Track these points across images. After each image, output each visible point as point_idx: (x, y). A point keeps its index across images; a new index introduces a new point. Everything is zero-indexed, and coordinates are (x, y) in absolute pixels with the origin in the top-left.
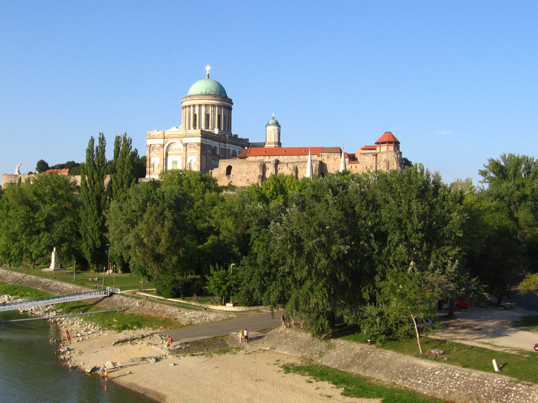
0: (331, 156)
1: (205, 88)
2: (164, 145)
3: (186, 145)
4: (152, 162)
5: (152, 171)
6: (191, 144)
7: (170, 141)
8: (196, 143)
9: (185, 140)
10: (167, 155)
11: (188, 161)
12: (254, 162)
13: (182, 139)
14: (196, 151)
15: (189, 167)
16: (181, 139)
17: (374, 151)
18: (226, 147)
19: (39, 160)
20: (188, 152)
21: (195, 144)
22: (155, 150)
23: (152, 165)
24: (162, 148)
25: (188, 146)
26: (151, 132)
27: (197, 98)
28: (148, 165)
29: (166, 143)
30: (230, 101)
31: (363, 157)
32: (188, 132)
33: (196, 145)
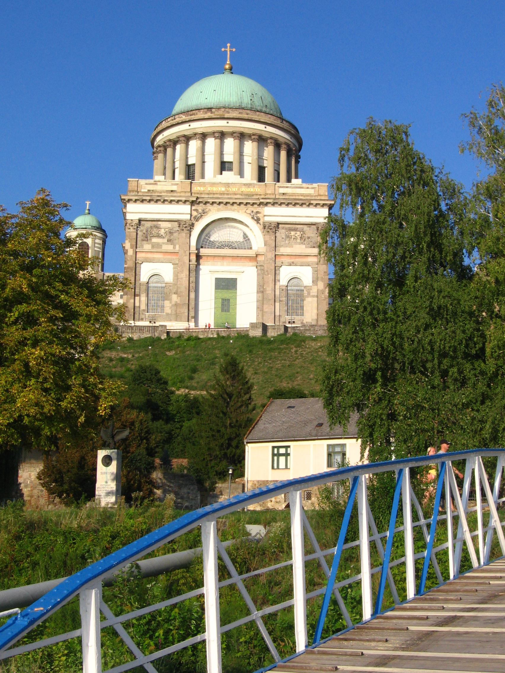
1: (249, 94)
2: (193, 225)
4: (144, 277)
5: (143, 307)
6: (293, 226)
7: (214, 214)
10: (198, 257)
11: (283, 280)
13: (259, 209)
15: (284, 299)
16: (256, 208)
20: (282, 250)
21: (305, 227)
22: (154, 240)
23: (144, 288)
24: (184, 234)
25: (281, 233)
26: (142, 182)
29: (197, 219)
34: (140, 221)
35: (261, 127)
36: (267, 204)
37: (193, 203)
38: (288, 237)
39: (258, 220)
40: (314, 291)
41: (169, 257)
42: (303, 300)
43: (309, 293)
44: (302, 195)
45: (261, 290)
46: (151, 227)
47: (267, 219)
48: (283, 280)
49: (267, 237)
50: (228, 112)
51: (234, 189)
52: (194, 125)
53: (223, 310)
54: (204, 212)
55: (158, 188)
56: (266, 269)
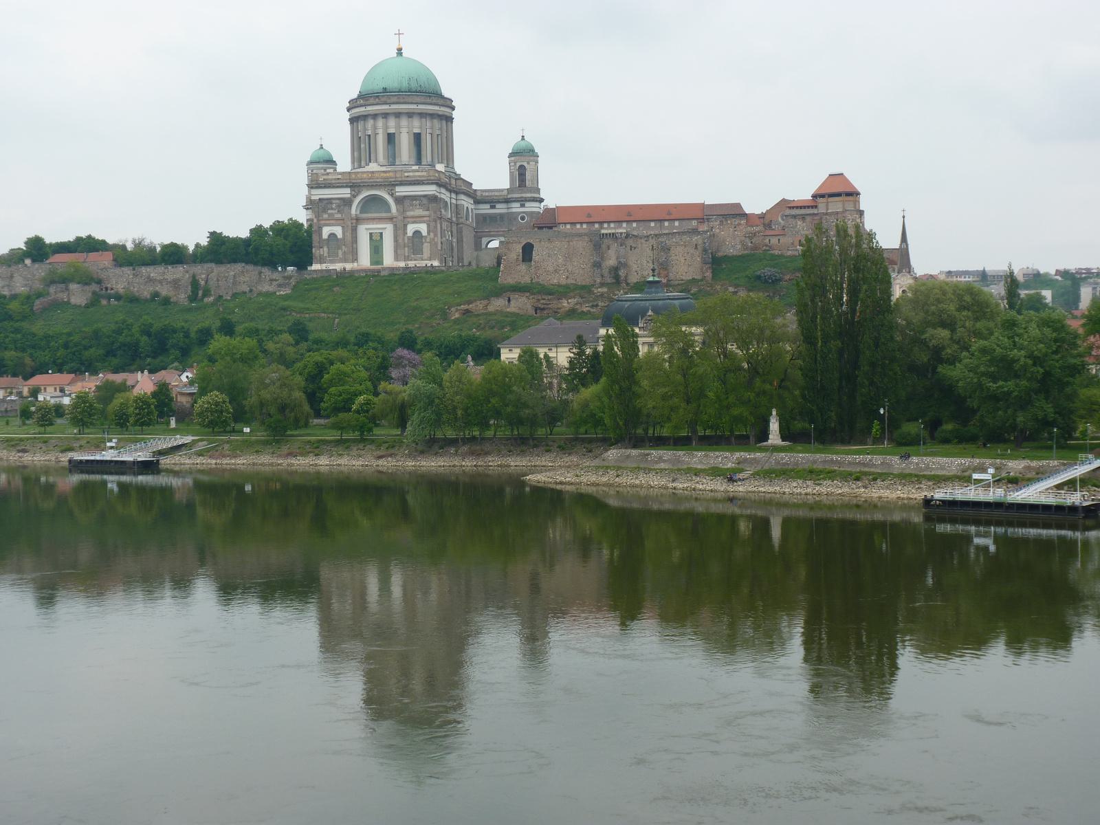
0: (727, 221)
3: (400, 200)
4: (325, 236)
5: (326, 254)
6: (413, 198)
7: (365, 193)
8: (425, 196)
9: (401, 191)
12: (580, 235)
14: (427, 213)
17: (815, 211)
18: (459, 202)
19: (32, 235)
22: (329, 211)
25: (407, 202)
27: (395, 99)
28: (315, 243)
29: (355, 196)
30: (448, 104)
31: (791, 221)
32: (406, 174)
33: (425, 201)
34: (320, 199)
35: (414, 106)
36: (397, 185)
37: (350, 187)
38: (412, 205)
39: (392, 195)
40: (428, 240)
41: (339, 222)
42: (423, 244)
43: (426, 240)
44: (419, 176)
45: (396, 240)
46: (327, 203)
47: (397, 194)
48: (410, 233)
49: (398, 206)
50: (390, 98)
51: (377, 175)
52: (369, 108)
53: (375, 253)
54: (359, 193)
55: (330, 177)
56: (398, 226)
